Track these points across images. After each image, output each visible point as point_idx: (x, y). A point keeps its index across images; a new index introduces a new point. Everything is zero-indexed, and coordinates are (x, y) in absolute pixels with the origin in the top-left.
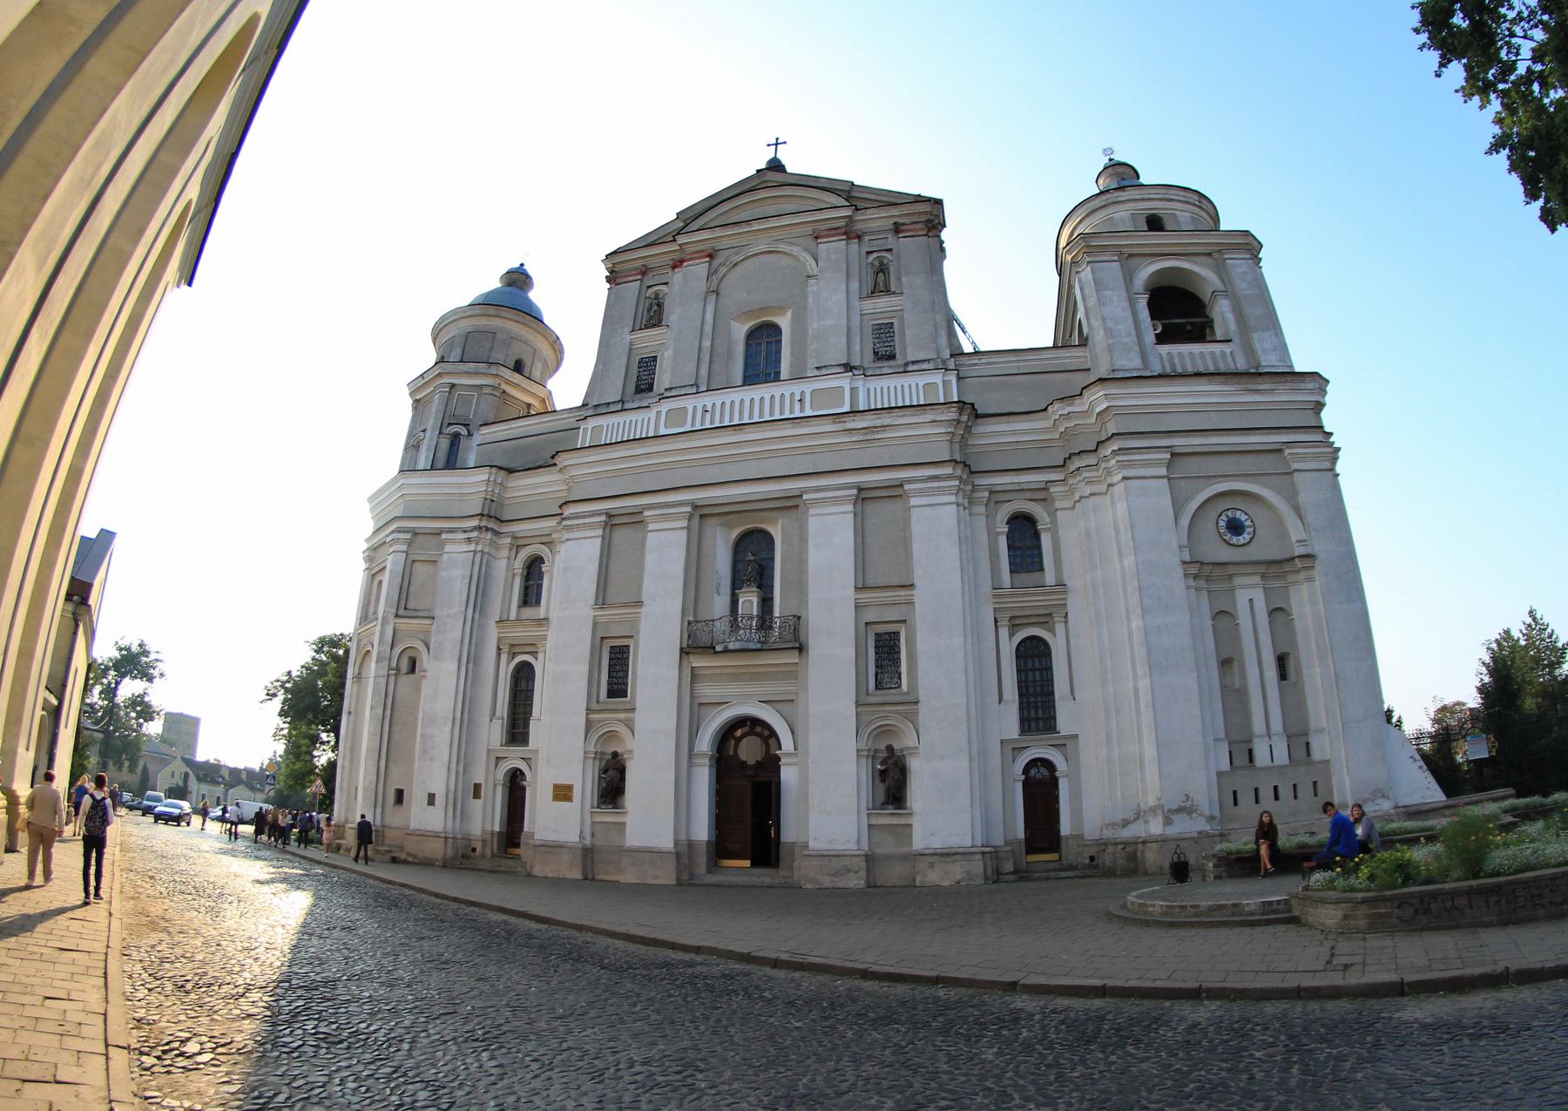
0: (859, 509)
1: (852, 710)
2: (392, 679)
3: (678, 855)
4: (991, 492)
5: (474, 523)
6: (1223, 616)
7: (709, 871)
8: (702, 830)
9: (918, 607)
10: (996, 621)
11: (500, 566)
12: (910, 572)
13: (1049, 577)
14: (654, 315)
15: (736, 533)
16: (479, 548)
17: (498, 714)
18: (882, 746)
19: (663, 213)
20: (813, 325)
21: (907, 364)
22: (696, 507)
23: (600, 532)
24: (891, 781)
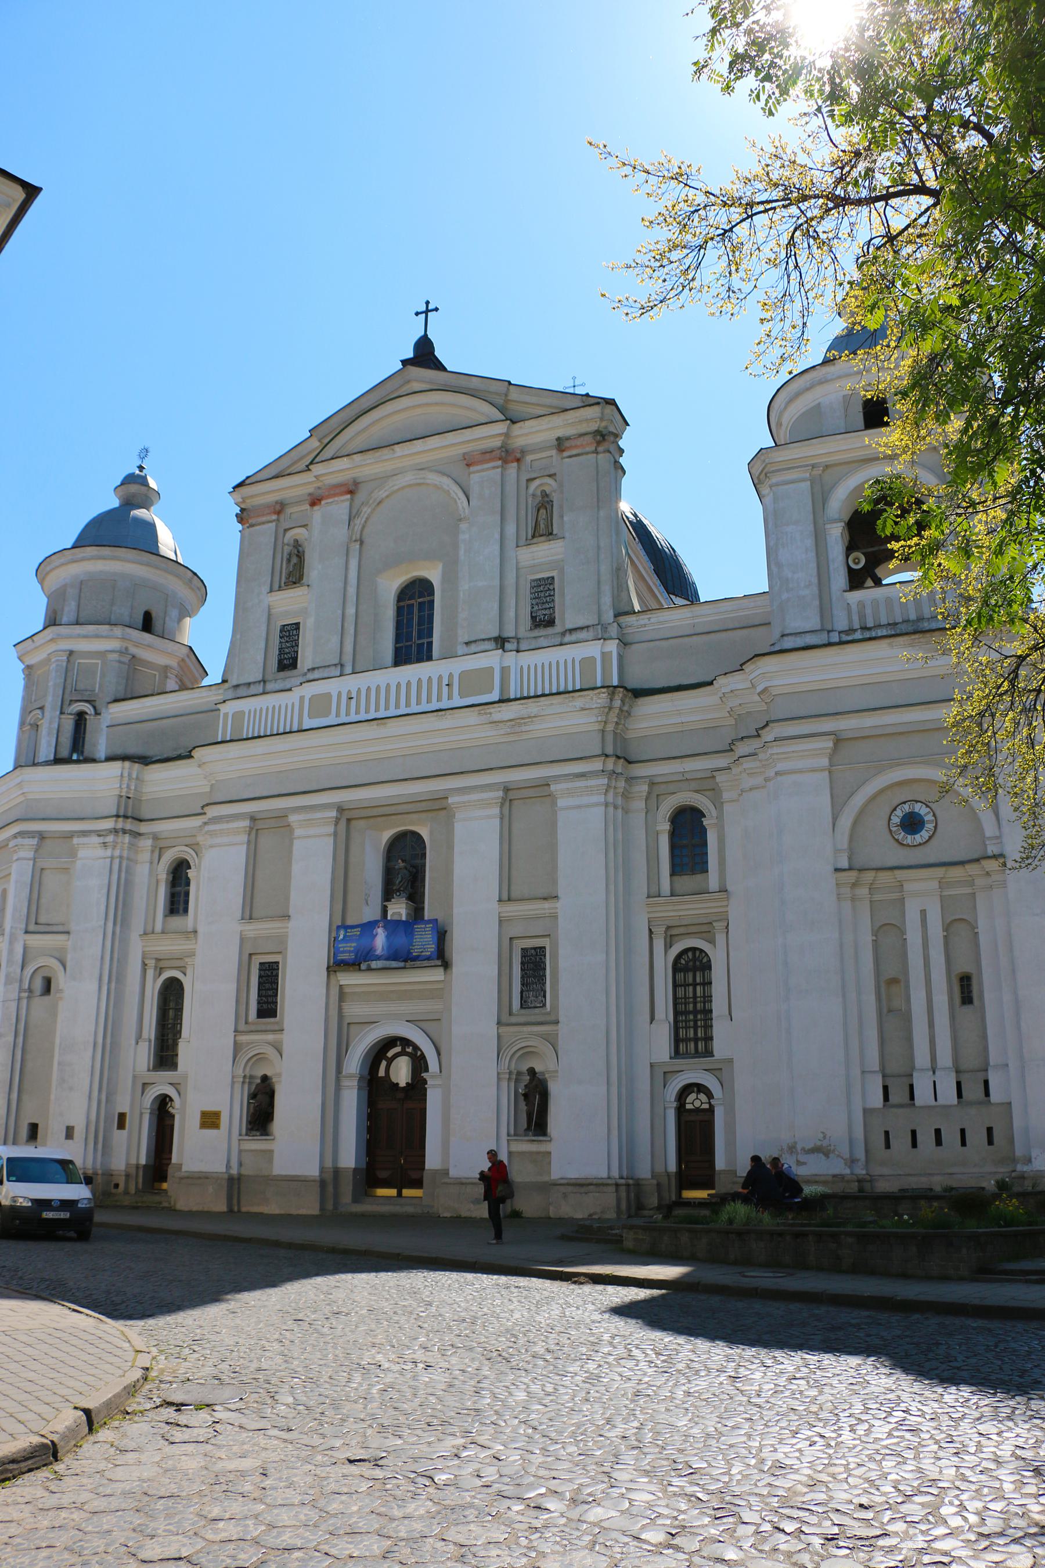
0: (506, 811)
1: (493, 1030)
2: (24, 1002)
3: (323, 1183)
4: (652, 784)
5: (109, 824)
6: (888, 933)
7: (356, 1200)
8: (349, 1157)
9: (560, 919)
10: (650, 930)
11: (142, 872)
12: (555, 882)
13: (713, 880)
14: (293, 570)
15: (387, 835)
16: (117, 853)
17: (145, 1034)
18: (524, 1068)
19: (292, 431)
20: (464, 586)
21: (563, 634)
22: (341, 810)
23: (244, 838)
24: (533, 1104)
